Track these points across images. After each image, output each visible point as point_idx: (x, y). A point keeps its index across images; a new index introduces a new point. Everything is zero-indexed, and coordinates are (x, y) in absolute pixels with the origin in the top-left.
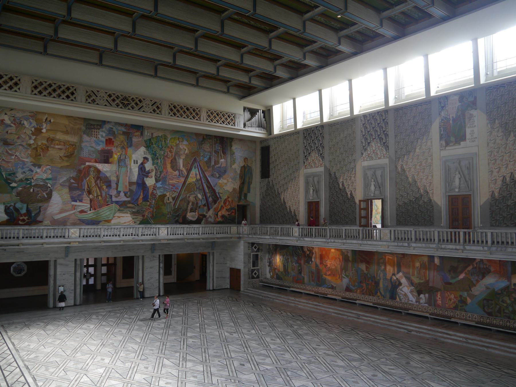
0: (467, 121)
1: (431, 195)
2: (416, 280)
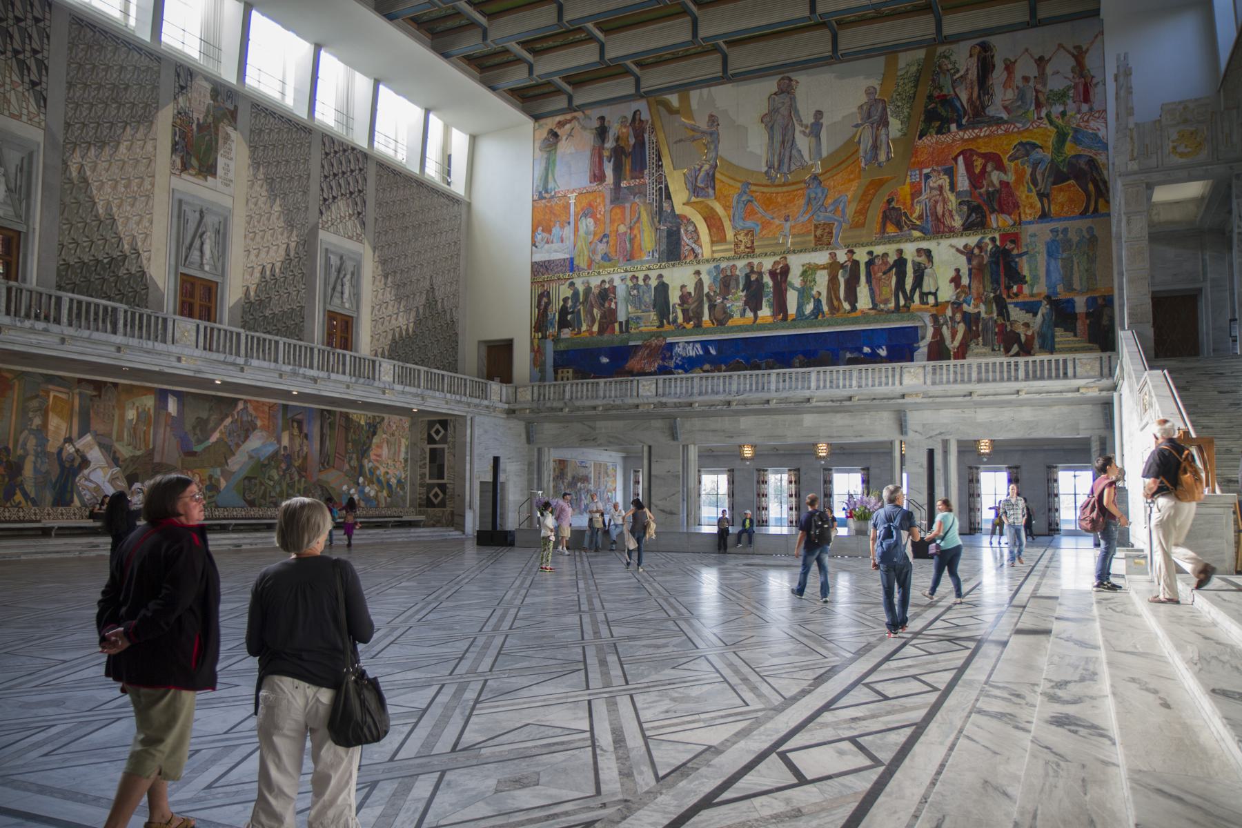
0: (221, 141)
1: (145, 262)
2: (125, 451)
